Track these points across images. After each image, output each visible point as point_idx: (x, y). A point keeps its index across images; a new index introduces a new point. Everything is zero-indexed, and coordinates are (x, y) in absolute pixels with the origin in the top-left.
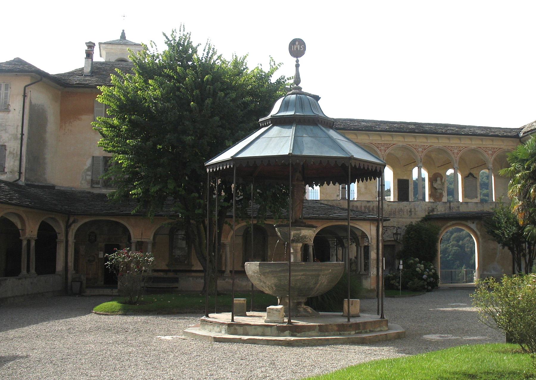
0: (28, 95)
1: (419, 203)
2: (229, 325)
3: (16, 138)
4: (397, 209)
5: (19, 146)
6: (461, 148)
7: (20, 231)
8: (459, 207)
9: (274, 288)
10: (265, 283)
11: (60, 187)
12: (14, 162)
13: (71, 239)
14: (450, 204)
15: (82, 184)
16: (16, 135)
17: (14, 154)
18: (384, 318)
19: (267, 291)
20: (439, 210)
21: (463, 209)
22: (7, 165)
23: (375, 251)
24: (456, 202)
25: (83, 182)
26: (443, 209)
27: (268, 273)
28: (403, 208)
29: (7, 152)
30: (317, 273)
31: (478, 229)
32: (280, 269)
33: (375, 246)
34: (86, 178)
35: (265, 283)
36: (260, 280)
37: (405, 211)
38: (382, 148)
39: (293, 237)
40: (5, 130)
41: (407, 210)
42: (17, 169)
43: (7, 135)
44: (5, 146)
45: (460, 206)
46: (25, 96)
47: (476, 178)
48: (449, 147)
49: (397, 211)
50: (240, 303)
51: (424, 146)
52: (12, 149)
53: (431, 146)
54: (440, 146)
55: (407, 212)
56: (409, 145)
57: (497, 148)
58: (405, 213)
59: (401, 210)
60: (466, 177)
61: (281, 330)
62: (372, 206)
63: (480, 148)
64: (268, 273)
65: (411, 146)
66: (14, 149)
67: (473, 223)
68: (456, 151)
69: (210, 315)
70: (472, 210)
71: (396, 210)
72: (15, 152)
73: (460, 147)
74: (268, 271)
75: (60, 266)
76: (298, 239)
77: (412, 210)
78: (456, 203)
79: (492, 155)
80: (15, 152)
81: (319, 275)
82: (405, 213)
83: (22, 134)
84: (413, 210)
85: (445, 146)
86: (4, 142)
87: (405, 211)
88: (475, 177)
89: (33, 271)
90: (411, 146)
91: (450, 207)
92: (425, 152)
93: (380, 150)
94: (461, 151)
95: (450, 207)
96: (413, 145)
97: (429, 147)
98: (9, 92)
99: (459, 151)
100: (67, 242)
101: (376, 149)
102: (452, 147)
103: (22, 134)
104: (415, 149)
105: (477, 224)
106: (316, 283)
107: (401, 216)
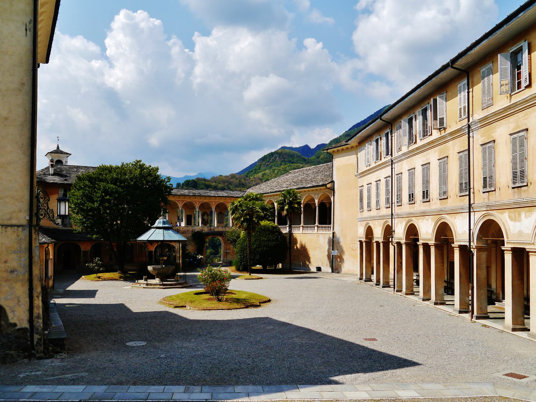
1: (196, 227)
2: (146, 284)
20: (205, 230)
21: (216, 230)
26: (207, 230)
31: (222, 240)
38: (180, 202)
47: (223, 214)
58: (190, 232)
59: (188, 231)
61: (160, 285)
62: (175, 229)
64: (156, 270)
67: (220, 237)
70: (220, 230)
76: (163, 260)
84: (193, 230)
91: (210, 229)
92: (200, 204)
93: (179, 203)
94: (216, 203)
95: (210, 229)
101: (177, 202)
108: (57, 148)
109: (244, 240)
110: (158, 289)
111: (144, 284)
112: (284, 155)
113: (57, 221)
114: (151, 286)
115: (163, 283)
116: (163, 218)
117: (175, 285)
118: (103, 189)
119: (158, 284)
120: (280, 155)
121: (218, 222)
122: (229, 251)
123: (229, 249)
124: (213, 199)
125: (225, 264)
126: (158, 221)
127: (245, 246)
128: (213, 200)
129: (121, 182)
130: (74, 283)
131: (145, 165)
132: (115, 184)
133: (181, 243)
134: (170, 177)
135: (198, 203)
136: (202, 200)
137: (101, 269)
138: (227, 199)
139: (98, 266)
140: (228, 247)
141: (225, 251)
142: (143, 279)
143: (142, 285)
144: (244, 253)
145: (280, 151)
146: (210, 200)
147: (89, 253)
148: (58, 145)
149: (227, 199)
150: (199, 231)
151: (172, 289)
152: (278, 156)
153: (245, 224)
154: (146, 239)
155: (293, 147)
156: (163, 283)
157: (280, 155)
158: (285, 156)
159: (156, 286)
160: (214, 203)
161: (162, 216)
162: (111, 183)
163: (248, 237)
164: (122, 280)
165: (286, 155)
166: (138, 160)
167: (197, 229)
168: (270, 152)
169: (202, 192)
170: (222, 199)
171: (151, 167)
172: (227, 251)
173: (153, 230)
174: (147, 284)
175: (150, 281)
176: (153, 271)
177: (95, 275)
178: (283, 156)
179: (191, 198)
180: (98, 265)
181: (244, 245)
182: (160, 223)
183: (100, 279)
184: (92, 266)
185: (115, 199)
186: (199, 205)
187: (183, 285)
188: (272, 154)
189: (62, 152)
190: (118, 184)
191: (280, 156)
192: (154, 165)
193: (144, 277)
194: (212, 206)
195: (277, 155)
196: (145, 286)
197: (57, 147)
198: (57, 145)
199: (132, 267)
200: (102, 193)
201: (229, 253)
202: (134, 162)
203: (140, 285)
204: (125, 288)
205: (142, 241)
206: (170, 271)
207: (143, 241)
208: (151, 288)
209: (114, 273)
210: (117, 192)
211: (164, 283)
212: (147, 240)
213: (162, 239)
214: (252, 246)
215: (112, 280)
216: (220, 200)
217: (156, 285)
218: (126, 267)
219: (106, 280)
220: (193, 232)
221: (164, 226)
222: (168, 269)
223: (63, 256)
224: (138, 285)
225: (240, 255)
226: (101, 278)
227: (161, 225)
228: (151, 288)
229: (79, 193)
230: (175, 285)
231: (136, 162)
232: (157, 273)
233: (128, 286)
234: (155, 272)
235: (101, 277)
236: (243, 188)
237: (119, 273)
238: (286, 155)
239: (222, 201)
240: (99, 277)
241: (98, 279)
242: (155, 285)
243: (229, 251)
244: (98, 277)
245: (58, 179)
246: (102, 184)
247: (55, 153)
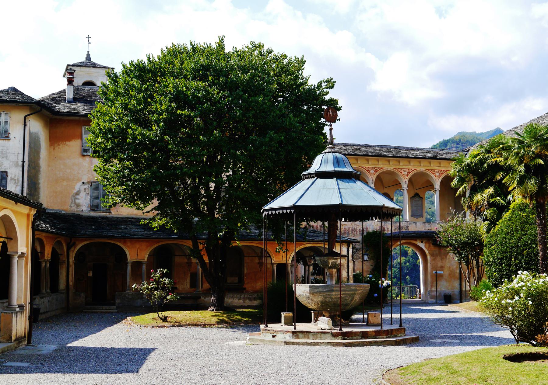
0: (28, 124)
3: (17, 165)
4: (350, 230)
5: (21, 173)
6: (410, 170)
7: (39, 254)
8: (408, 227)
9: (320, 304)
10: (312, 300)
11: (55, 210)
12: (16, 188)
13: (72, 260)
14: (400, 224)
15: (71, 207)
16: (17, 162)
17: (15, 180)
18: (402, 327)
19: (312, 306)
23: (346, 270)
24: (406, 222)
25: (72, 205)
27: (316, 293)
28: (356, 228)
29: (9, 179)
30: (353, 292)
31: (426, 248)
32: (327, 289)
33: (346, 266)
34: (75, 201)
35: (312, 300)
36: (308, 298)
37: (358, 230)
39: (332, 264)
40: (6, 157)
41: (360, 229)
43: (9, 162)
44: (6, 172)
45: (409, 226)
46: (25, 125)
47: (422, 198)
48: (399, 169)
49: (350, 230)
50: (289, 316)
51: (376, 168)
52: (13, 176)
53: (382, 168)
54: (391, 168)
55: (360, 231)
56: (362, 167)
57: (444, 170)
58: (358, 232)
60: (413, 197)
61: (335, 335)
63: (428, 170)
64: (316, 293)
65: (364, 168)
66: (15, 176)
67: (422, 242)
68: (405, 173)
69: (269, 325)
70: (420, 230)
71: (349, 229)
72: (16, 178)
73: (409, 169)
74: (316, 291)
75: (62, 285)
77: (364, 230)
78: (405, 223)
79: (439, 176)
80: (16, 178)
81: (355, 294)
82: (358, 232)
83: (24, 162)
85: (395, 169)
86: (5, 169)
87: (358, 230)
88: (421, 197)
89: (49, 291)
90: (364, 168)
92: (377, 173)
94: (410, 173)
96: (365, 167)
97: (380, 169)
98: (9, 121)
99: (409, 173)
100: (68, 262)
102: (401, 169)
103: (24, 162)
104: (367, 171)
105: (425, 243)
106: (352, 300)
107: (354, 235)
108: (86, 58)
109: (507, 234)
110: (329, 347)
111: (286, 332)
112: (465, 143)
113: (78, 199)
114: (308, 338)
115: (341, 330)
116: (333, 150)
117: (377, 334)
118: (174, 91)
119: (327, 333)
120: (458, 144)
121: (412, 215)
122: (442, 272)
123: (442, 268)
124: (403, 165)
125: (434, 301)
126: (318, 159)
127: (512, 248)
128: (404, 165)
129: (218, 73)
130: (99, 330)
131: (272, 51)
132: (204, 78)
133: (351, 247)
134: (332, 79)
135: (372, 172)
136: (382, 166)
137: (169, 297)
138: (434, 163)
139: (163, 289)
140: (440, 264)
141: (434, 272)
142: (280, 322)
143: (280, 337)
144: (510, 265)
145: (457, 138)
146: (397, 167)
147: (144, 267)
148: (88, 52)
149: (432, 165)
150: (377, 231)
151: (365, 348)
152: (455, 146)
153: (533, 181)
154: (290, 204)
155: (477, 132)
156: (341, 330)
157: (458, 144)
158: (465, 145)
159: (321, 338)
160: (405, 173)
161: (330, 146)
162: (194, 79)
163: (539, 216)
164: (223, 328)
165: (468, 144)
166: (257, 42)
167: (371, 226)
168: (441, 140)
169: (381, 150)
170: (422, 165)
171: (288, 58)
172: (438, 272)
173: (306, 183)
174: (295, 333)
175: (301, 327)
176: (308, 298)
177: (155, 315)
178: (463, 146)
179: (359, 162)
180: (160, 286)
181: (510, 243)
182: (327, 162)
183: (166, 324)
184: (148, 288)
185: (203, 115)
186: (375, 176)
187: (396, 336)
188: (445, 144)
189: (95, 66)
190: (210, 78)
191: (458, 146)
192: (292, 53)
193: (283, 315)
194: (403, 178)
195: (452, 145)
196: (288, 338)
197: (85, 56)
198: (87, 53)
199: (241, 301)
200: (171, 102)
201: (441, 275)
202: (247, 47)
203: (274, 337)
204: (232, 343)
205: (277, 212)
206: (357, 298)
207: (281, 212)
208: (307, 344)
209: (200, 311)
210: (208, 98)
211: (344, 330)
212: (294, 207)
213: (337, 202)
214: (532, 247)
215: (196, 325)
216: (418, 166)
217: (323, 335)
218: (231, 300)
219: (181, 326)
220: (365, 234)
221: (337, 169)
222: (353, 290)
223: (90, 274)
224: (269, 337)
225: (500, 270)
226: (169, 320)
227: (330, 168)
228: (307, 344)
229: (115, 109)
230: (377, 334)
231: (250, 46)
232: (322, 302)
233: (237, 339)
234: (315, 300)
235: (171, 318)
236: (400, 196)
237: (213, 310)
238: (468, 144)
239: (422, 169)
240: (165, 319)
241: (161, 323)
242: (319, 335)
243: (442, 272)
244: (161, 319)
245: (81, 108)
246: (171, 83)
247: (81, 66)
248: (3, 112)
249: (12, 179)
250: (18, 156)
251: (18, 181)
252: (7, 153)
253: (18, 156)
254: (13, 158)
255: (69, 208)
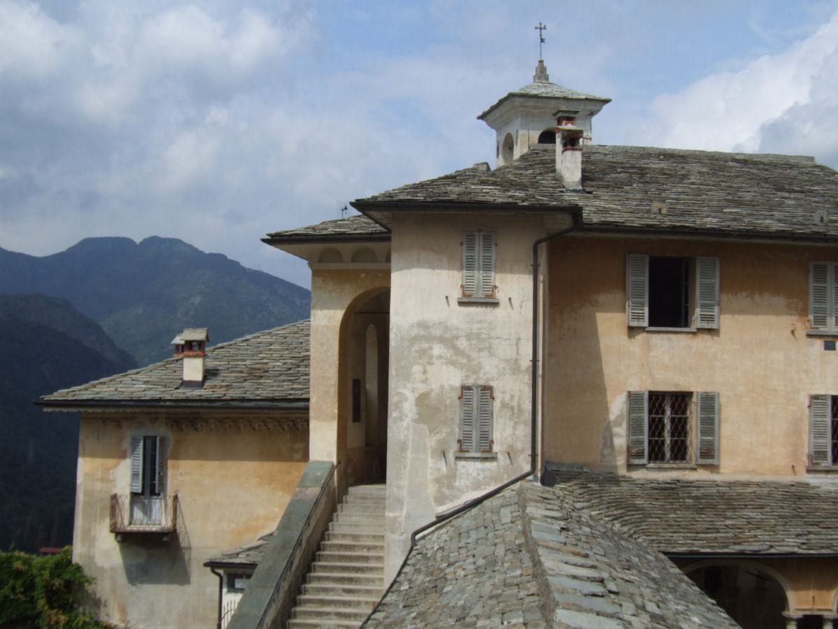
3: (515, 369)
12: (514, 428)
16: (517, 360)
17: (512, 408)
22: (496, 435)
29: (497, 404)
40: (490, 348)
42: (523, 443)
43: (495, 361)
66: (512, 397)
72: (515, 403)
80: (515, 403)
86: (488, 380)
103: (535, 361)
248: (480, 231)
249: (504, 405)
250: (517, 345)
251: (520, 410)
252: (490, 337)
253: (517, 345)
254: (504, 350)
255: (599, 458)
